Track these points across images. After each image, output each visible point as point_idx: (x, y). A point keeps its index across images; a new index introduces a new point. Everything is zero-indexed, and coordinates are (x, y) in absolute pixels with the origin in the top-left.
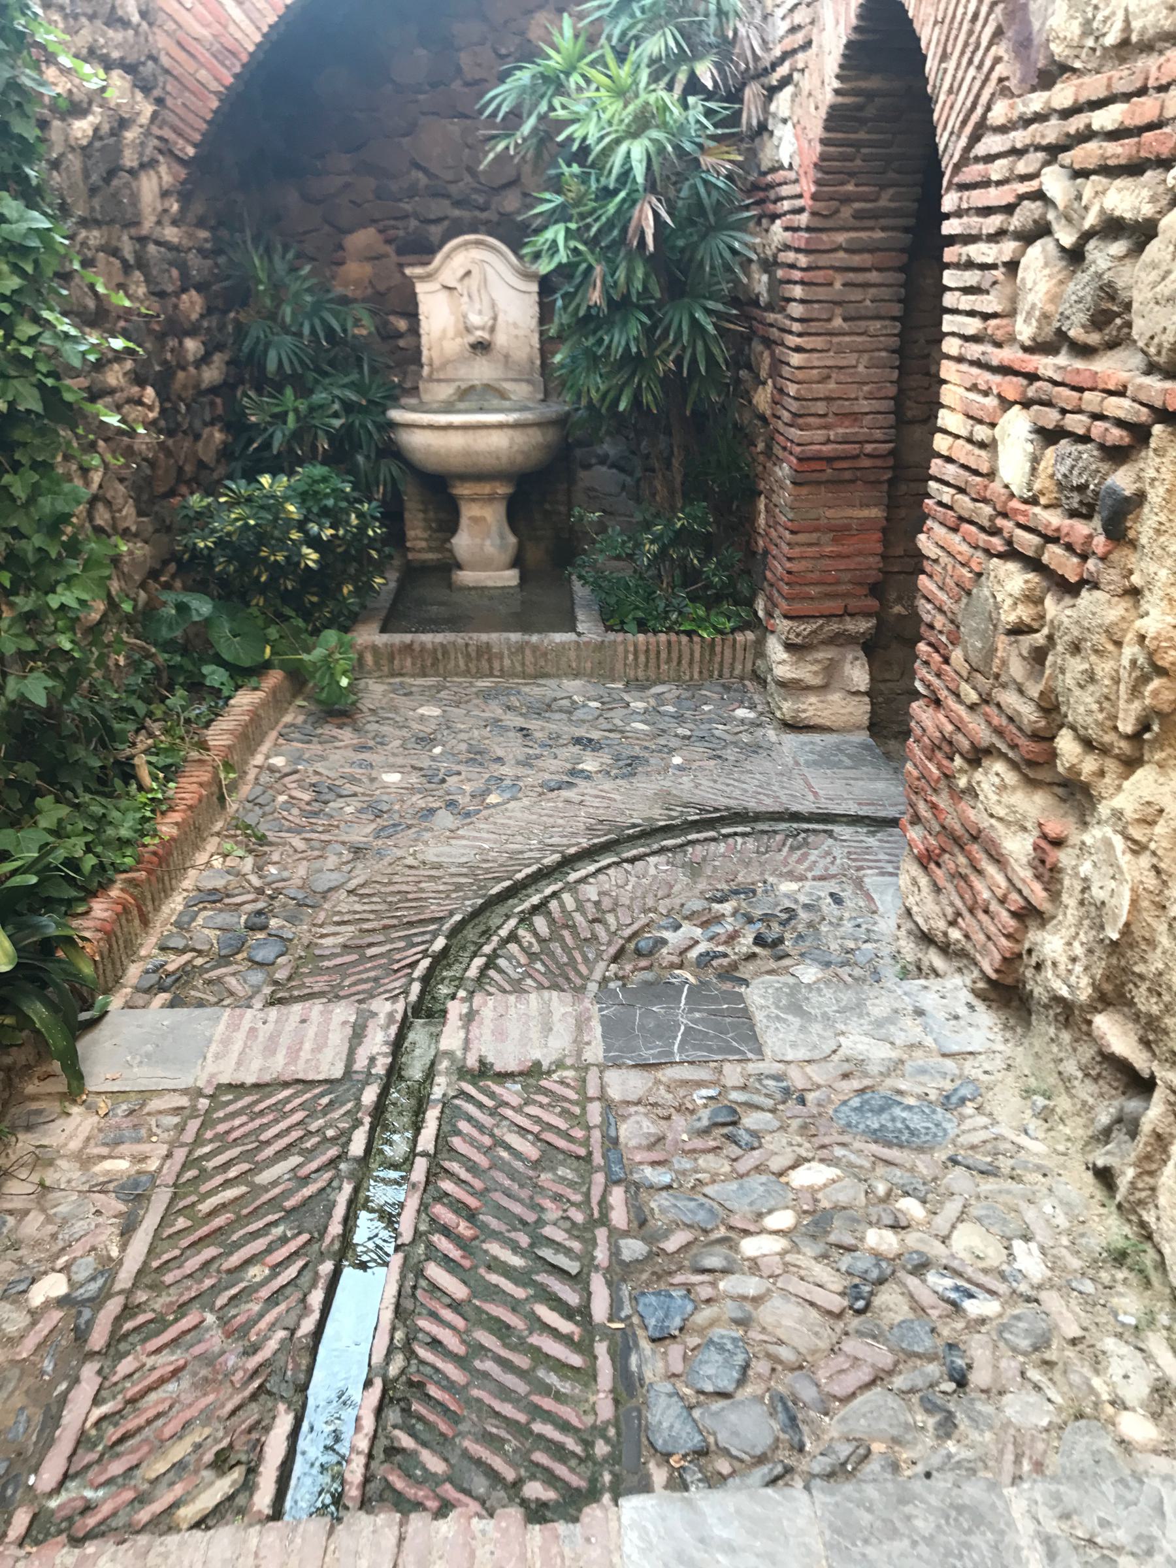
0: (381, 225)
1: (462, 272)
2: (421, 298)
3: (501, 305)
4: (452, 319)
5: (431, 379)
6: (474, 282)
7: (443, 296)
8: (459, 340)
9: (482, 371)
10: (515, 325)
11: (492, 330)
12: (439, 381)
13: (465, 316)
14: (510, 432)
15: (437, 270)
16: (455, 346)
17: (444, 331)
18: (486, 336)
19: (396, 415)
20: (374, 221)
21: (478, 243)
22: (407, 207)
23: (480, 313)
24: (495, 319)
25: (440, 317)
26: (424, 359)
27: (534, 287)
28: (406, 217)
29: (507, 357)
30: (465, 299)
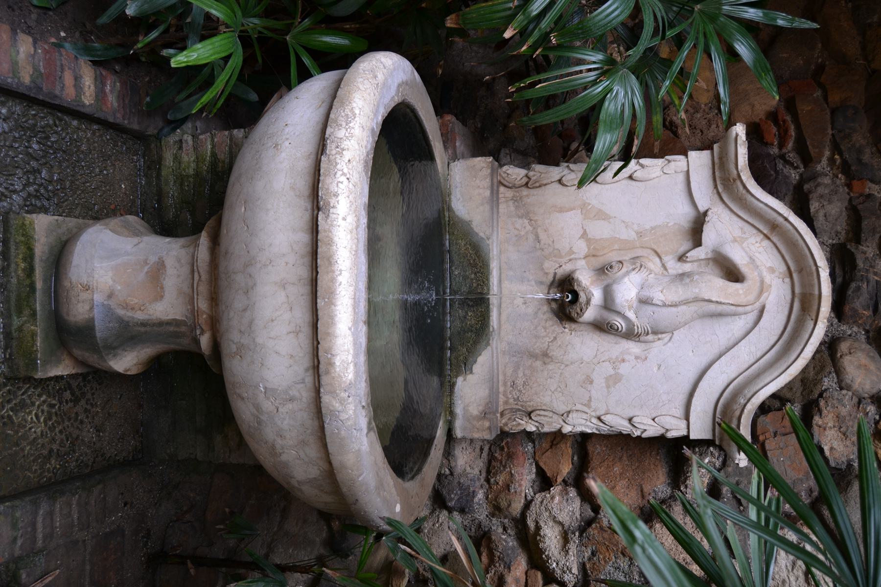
1: (738, 257)
2: (678, 162)
3: (659, 349)
4: (627, 234)
5: (497, 184)
6: (715, 287)
8: (581, 248)
10: (614, 380)
11: (602, 327)
13: (637, 263)
14: (304, 394)
17: (602, 215)
18: (589, 314)
20: (789, 104)
21: (804, 304)
22: (823, 165)
23: (644, 301)
24: (631, 334)
27: (700, 430)
28: (807, 159)
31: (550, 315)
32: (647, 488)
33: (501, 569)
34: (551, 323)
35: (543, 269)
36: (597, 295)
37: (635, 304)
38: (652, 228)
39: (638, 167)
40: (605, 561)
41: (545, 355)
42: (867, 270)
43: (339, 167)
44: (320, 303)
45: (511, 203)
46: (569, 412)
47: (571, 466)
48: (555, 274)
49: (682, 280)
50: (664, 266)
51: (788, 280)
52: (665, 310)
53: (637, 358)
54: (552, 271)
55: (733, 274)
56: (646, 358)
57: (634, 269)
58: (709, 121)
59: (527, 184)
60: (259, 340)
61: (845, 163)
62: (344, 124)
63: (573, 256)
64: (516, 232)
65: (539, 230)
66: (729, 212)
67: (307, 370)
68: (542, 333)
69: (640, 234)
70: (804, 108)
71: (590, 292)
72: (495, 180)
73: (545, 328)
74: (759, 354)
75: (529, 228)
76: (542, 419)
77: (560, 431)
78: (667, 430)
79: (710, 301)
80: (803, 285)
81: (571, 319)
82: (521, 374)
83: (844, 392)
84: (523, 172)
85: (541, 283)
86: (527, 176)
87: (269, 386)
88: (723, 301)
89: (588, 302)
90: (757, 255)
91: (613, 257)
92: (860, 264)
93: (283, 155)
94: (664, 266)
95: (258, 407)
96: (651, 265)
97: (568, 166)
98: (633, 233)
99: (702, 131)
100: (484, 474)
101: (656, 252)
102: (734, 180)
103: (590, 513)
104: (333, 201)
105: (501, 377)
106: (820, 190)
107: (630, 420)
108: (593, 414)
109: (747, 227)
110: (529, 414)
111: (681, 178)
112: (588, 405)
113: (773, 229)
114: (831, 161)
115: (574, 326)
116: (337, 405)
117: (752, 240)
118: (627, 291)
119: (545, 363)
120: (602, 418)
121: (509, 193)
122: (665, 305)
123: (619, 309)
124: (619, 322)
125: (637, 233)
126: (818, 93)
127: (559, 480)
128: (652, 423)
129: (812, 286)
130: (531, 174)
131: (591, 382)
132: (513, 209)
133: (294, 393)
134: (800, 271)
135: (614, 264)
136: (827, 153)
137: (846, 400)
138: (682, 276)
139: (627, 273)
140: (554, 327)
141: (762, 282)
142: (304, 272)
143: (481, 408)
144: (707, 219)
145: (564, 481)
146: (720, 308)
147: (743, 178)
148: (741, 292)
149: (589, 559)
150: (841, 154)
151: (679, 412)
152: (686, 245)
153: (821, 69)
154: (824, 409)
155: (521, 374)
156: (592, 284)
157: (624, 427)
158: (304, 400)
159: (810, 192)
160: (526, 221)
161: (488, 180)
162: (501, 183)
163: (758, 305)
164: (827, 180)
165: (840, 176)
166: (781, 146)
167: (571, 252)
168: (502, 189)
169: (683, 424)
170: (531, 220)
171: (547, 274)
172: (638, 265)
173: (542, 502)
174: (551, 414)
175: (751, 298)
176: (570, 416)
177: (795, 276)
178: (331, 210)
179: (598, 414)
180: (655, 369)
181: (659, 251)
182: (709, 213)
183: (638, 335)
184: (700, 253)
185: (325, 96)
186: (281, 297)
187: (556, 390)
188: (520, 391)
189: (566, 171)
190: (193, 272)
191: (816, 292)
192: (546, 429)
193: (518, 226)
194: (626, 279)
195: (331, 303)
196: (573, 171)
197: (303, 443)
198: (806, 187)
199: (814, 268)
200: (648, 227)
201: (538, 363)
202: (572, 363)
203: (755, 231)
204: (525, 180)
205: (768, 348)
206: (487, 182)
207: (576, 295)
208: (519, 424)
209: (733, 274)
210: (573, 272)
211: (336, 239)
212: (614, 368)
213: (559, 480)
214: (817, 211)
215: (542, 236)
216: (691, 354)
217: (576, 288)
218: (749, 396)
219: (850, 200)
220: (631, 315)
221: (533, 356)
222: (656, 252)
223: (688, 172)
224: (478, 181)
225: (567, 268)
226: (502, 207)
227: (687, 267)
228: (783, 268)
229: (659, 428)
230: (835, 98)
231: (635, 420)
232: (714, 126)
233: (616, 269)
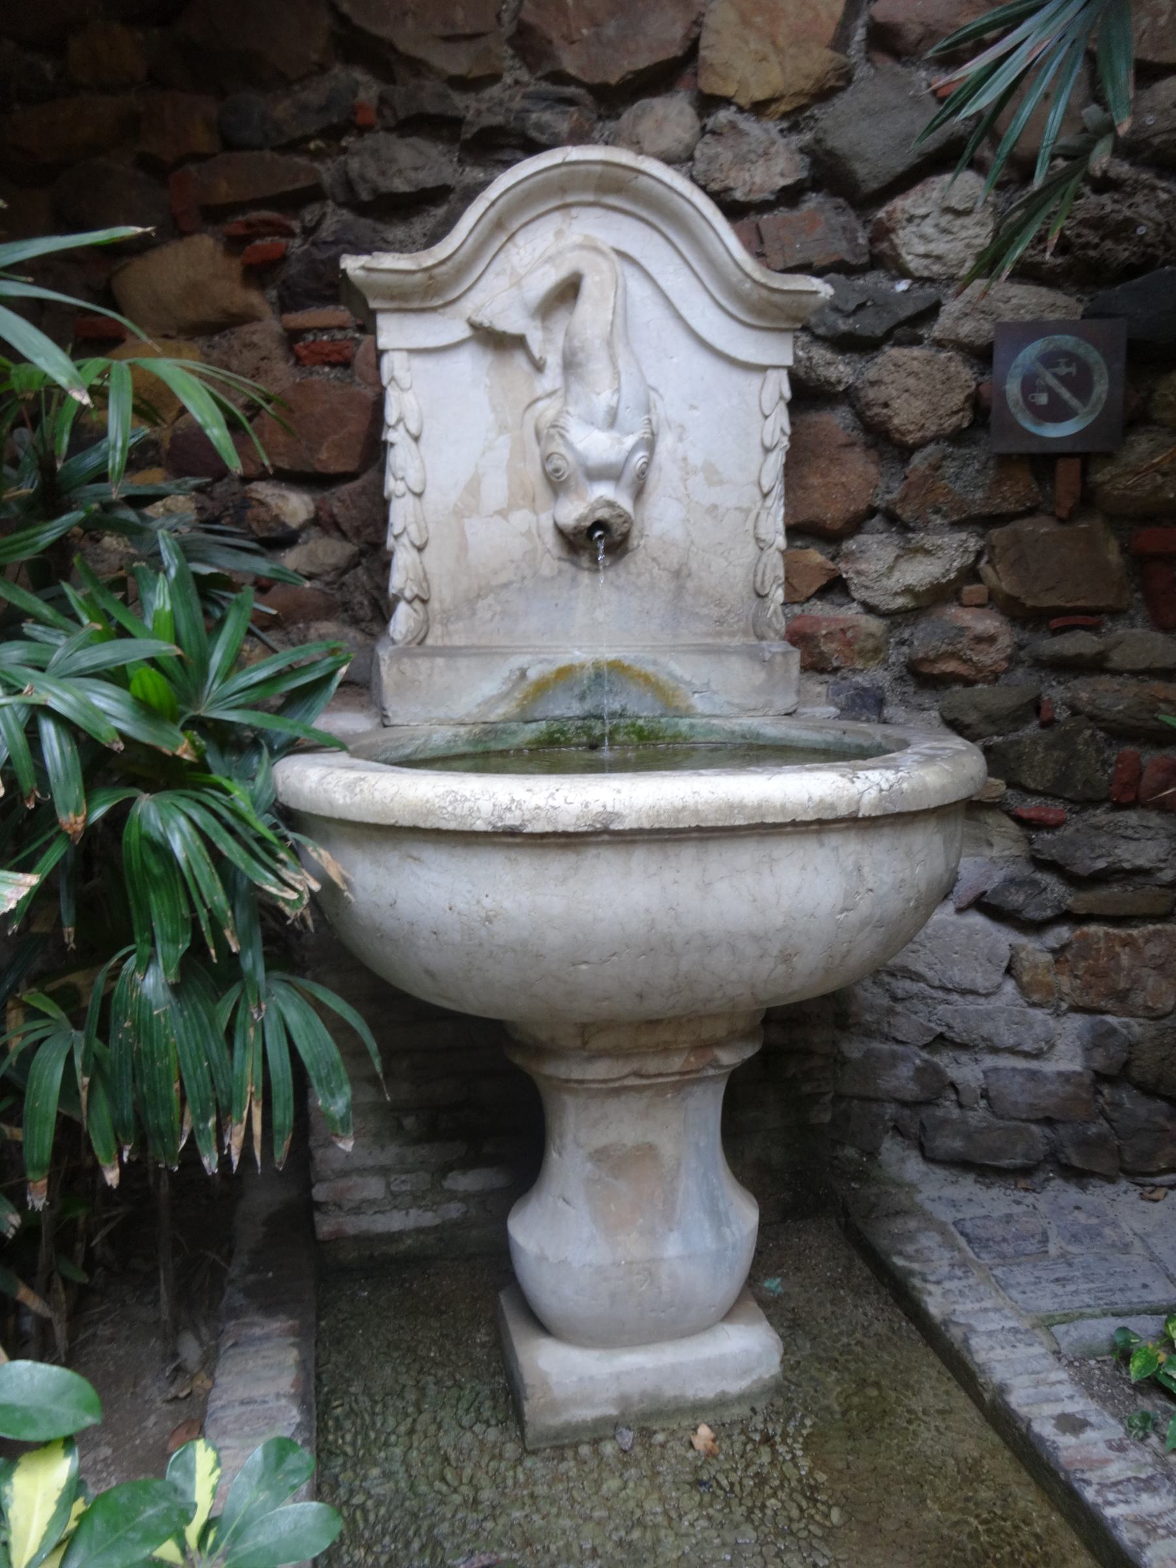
0: (235, 225)
1: (547, 279)
2: (394, 366)
3: (669, 408)
4: (503, 446)
6: (591, 315)
7: (470, 366)
8: (521, 518)
9: (593, 627)
11: (639, 492)
12: (450, 652)
15: (461, 268)
16: (515, 534)
17: (473, 487)
18: (625, 503)
19: (315, 780)
20: (213, 215)
21: (612, 189)
23: (612, 420)
24: (650, 444)
25: (453, 437)
26: (398, 580)
28: (315, 194)
29: (679, 574)
30: (552, 378)
31: (620, 567)
32: (842, 439)
33: (965, 640)
34: (632, 567)
35: (553, 578)
36: (603, 490)
37: (615, 434)
38: (494, 410)
39: (401, 427)
40: (949, 493)
41: (677, 574)
42: (508, 110)
43: (542, 803)
44: (740, 821)
45: (451, 627)
46: (758, 540)
47: (811, 550)
48: (560, 559)
49: (580, 365)
50: (550, 395)
51: (574, 212)
52: (625, 389)
53: (681, 439)
54: (556, 564)
55: (568, 291)
56: (682, 426)
57: (562, 436)
58: (245, 346)
59: (424, 602)
60: (779, 921)
61: (324, 134)
62: (467, 805)
63: (534, 531)
64: (497, 618)
65: (494, 583)
66: (473, 293)
67: (822, 845)
68: (645, 579)
69: (503, 428)
70: (224, 191)
71: (597, 501)
72: (419, 650)
73: (639, 575)
74: (677, 260)
75: (491, 599)
76: (769, 577)
77: (783, 553)
78: (782, 397)
79: (612, 324)
80: (584, 189)
81: (626, 536)
82: (705, 611)
83: (697, 154)
84: (402, 609)
85: (574, 580)
86: (410, 602)
87: (839, 907)
88: (611, 305)
89: (611, 504)
90: (537, 254)
91: (533, 472)
92: (497, 120)
93: (507, 904)
94: (550, 395)
95: (864, 924)
96: (551, 414)
97: (396, 537)
98: (502, 439)
99: (263, 359)
100: (826, 677)
101: (530, 406)
102: (431, 278)
103: (877, 522)
104: (596, 808)
105: (709, 641)
106: (372, 173)
107: (767, 450)
108: (759, 504)
109: (496, 266)
110: (761, 596)
111: (418, 362)
112: (747, 512)
113: (501, 226)
114: (317, 155)
115: (635, 532)
116: (874, 793)
117: (515, 259)
118: (594, 443)
119: (689, 575)
120: (765, 490)
121: (437, 630)
122: (618, 390)
123: (624, 455)
124: (639, 458)
125: (500, 433)
126: (192, 168)
127: (831, 565)
128: (771, 419)
129: (589, 174)
130: (408, 594)
131: (715, 507)
132: (460, 625)
133: (849, 864)
134: (563, 190)
135: (549, 468)
136: (302, 161)
137: (711, 151)
138: (571, 365)
139: (569, 445)
140: (638, 560)
141: (582, 247)
142: (688, 853)
143: (757, 667)
144: (486, 324)
145: (833, 559)
146: (619, 310)
147: (430, 262)
148: (597, 278)
149: (945, 516)
150: (307, 139)
151: (755, 380)
152: (520, 360)
153: (146, 163)
154: (723, 184)
155: (705, 611)
156: (583, 499)
157: (777, 460)
158: (859, 848)
159: (374, 190)
160: (480, 604)
161: (419, 661)
162: (421, 643)
163: (614, 256)
164: (354, 165)
165: (343, 143)
166: (290, 234)
167: (528, 534)
168: (429, 641)
169: (773, 375)
170: (479, 596)
171: (560, 572)
172: (552, 431)
173: (867, 588)
174: (761, 566)
175: (604, 265)
176: (763, 537)
177: (570, 199)
178: (609, 809)
179: (759, 497)
180: (696, 413)
181: (528, 401)
182: (478, 319)
183: (653, 434)
184: (535, 338)
185: (392, 857)
186: (722, 888)
187: (726, 559)
188: (729, 612)
189: (404, 540)
190: (617, 1092)
191: (599, 168)
192: (781, 573)
193: (489, 615)
194: (580, 446)
195: (741, 807)
196: (405, 529)
197: (909, 854)
198: (365, 196)
199: (564, 169)
200: (492, 417)
201: (690, 585)
202: (689, 535)
203: (502, 256)
204: (417, 605)
205: (669, 248)
206: (424, 664)
207: (599, 524)
208: (775, 612)
209: (568, 291)
210: (560, 531)
211: (650, 801)
212: (695, 473)
213: (831, 565)
214: (409, 182)
215: (503, 578)
216: (675, 360)
217: (588, 524)
218: (740, 275)
219: (388, 130)
220: (630, 441)
221: (680, 591)
222: (530, 406)
223: (413, 352)
224: (421, 678)
225: (551, 539)
226: (458, 641)
227: (553, 361)
228: (556, 219)
229: (777, 409)
230: (202, 140)
231: (768, 443)
232: (255, 338)
233: (559, 463)
